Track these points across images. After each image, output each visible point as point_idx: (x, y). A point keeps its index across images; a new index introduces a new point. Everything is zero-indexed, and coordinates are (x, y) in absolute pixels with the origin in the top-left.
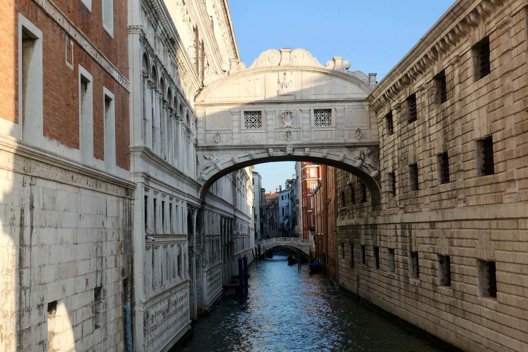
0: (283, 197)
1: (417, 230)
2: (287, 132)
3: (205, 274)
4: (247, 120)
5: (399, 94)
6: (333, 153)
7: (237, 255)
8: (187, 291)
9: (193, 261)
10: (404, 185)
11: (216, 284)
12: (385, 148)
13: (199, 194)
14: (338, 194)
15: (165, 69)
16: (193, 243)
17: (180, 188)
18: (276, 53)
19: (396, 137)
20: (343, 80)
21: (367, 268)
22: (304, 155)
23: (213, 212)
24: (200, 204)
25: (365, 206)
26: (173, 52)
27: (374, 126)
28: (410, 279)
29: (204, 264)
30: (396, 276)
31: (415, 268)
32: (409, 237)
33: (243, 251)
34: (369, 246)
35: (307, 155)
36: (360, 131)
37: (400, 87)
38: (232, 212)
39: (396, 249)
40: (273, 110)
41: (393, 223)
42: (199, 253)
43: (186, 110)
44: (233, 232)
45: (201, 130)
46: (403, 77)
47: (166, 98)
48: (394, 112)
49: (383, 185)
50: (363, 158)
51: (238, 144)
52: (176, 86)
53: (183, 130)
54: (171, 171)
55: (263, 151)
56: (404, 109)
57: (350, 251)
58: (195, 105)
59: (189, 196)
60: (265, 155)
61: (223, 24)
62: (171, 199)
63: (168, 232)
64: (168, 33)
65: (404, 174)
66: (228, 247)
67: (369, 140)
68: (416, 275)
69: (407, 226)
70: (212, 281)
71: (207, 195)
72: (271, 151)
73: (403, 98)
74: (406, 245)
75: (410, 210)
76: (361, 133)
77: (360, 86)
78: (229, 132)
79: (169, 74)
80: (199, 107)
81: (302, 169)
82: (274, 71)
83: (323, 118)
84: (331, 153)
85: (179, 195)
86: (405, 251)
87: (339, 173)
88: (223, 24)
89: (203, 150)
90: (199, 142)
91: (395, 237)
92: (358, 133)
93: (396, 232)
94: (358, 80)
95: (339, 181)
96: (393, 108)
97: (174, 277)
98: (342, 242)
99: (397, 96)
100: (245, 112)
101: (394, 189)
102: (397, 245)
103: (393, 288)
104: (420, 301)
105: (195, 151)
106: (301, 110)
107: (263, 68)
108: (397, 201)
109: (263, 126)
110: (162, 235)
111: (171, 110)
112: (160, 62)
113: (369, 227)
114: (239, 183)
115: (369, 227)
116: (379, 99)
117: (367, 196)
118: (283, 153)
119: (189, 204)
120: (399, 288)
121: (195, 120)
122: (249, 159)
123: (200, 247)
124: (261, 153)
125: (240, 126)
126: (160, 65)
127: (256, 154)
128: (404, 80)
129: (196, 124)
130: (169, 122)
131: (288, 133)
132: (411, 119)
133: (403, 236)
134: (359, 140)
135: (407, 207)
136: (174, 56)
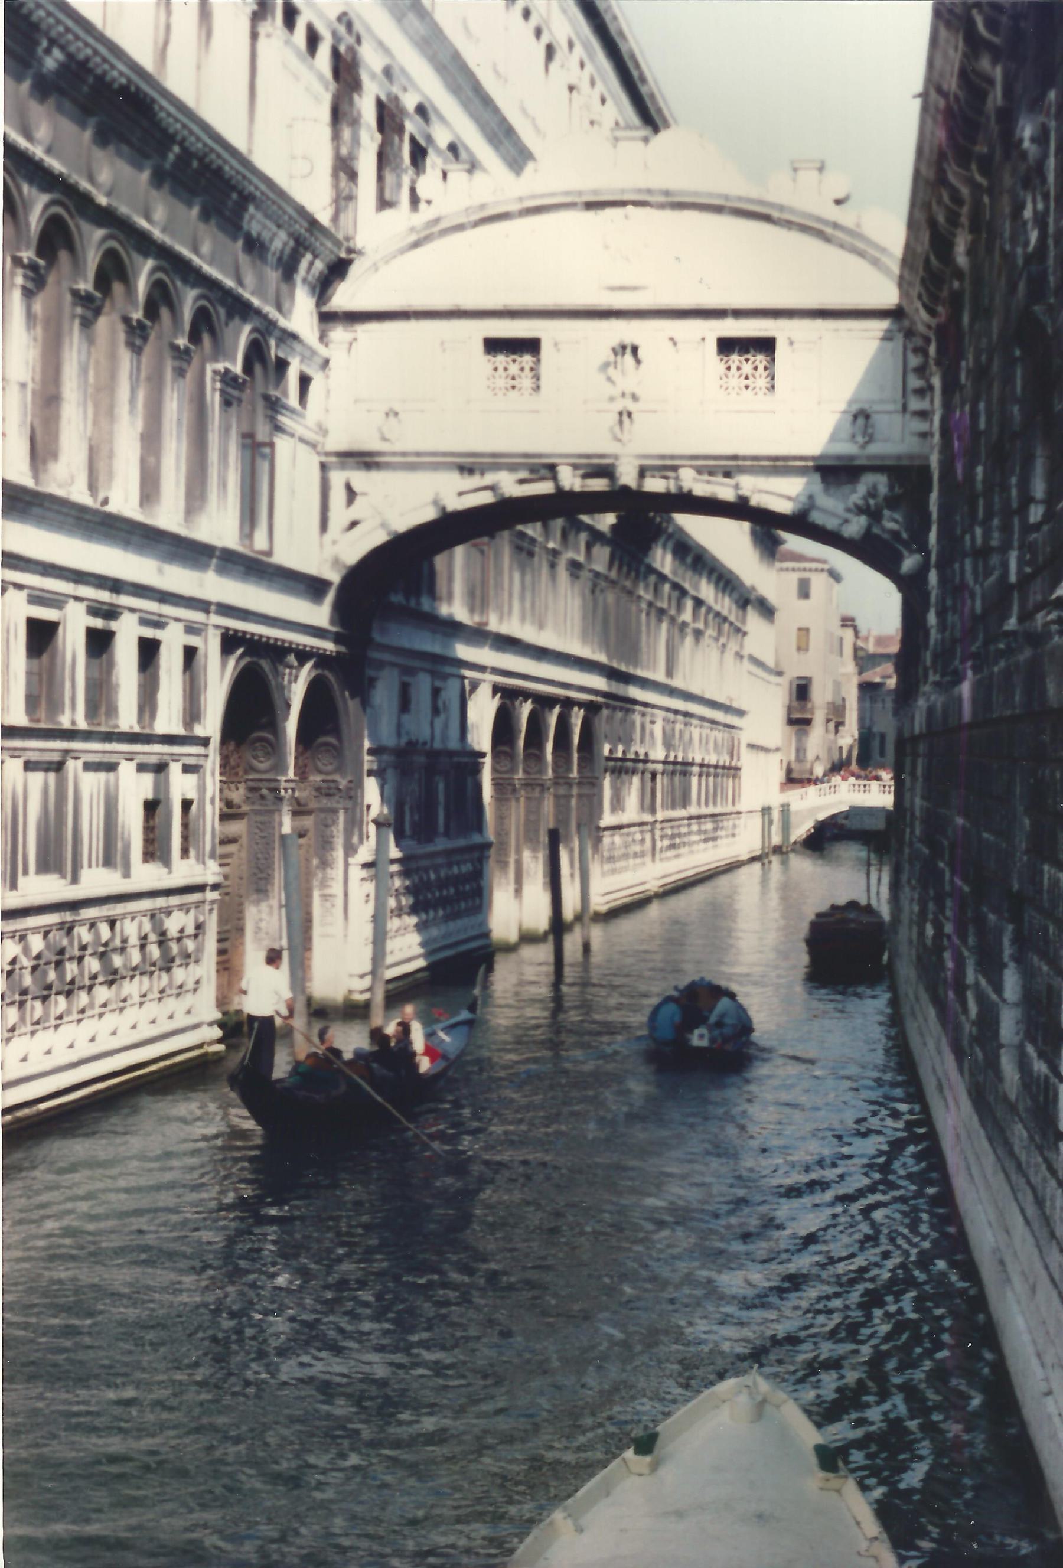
2: (621, 414)
29: (355, 840)
36: (867, 417)
38: (599, 682)
43: (247, 329)
44: (601, 749)
50: (873, 508)
59: (227, 610)
60: (545, 487)
61: (578, 50)
64: (99, 71)
82: (590, 206)
83: (747, 368)
88: (578, 50)
92: (861, 421)
106: (672, 339)
114: (667, 587)
127: (511, 486)
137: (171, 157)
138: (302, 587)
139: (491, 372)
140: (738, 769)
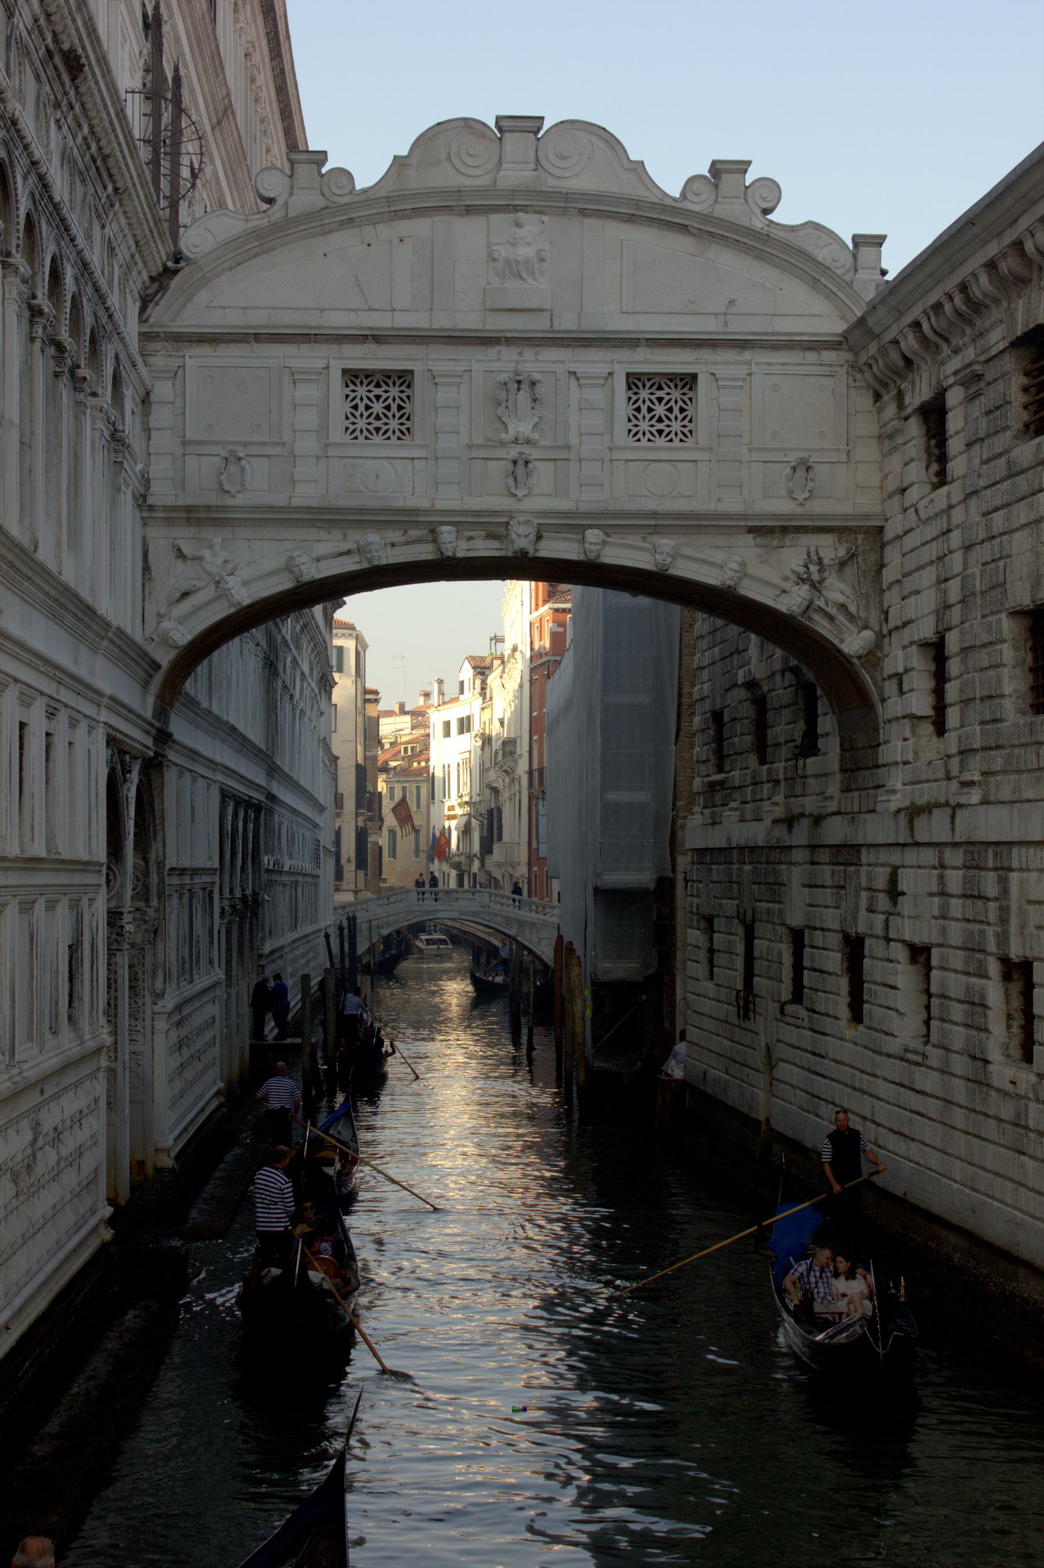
0: (447, 725)
1: (1035, 874)
2: (515, 462)
3: (161, 1025)
4: (356, 407)
5: (979, 322)
6: (698, 555)
7: (272, 952)
8: (99, 1088)
9: (120, 971)
10: (986, 693)
11: (199, 1066)
12: (909, 542)
13: (151, 700)
14: (697, 720)
15: (41, 177)
16: (120, 896)
17: (83, 673)
18: (483, 136)
19: (957, 496)
20: (750, 259)
21: (810, 1019)
22: (582, 557)
23: (196, 776)
24: (150, 742)
25: (809, 772)
26: (71, 107)
27: (868, 452)
28: (991, 1067)
29: (159, 984)
30: (935, 1056)
31: (1015, 1023)
32: (996, 899)
33: (296, 935)
34: (822, 929)
35: (592, 556)
36: (808, 469)
37: (985, 295)
38: (260, 777)
39: (939, 945)
40: (459, 367)
41: (929, 844)
42: (139, 938)
43: (111, 354)
45: (162, 441)
46: (1004, 256)
47: (42, 300)
48: (954, 397)
49: (890, 688)
50: (816, 577)
51: (314, 503)
52: (79, 253)
53: (98, 434)
54: (56, 601)
55: (414, 533)
56: (1000, 385)
57: (740, 948)
58: (145, 337)
59: (116, 705)
60: (424, 552)
62: (51, 715)
63: (39, 849)
64: (59, 28)
65: (984, 646)
66: (243, 918)
67: (846, 508)
68: (1016, 1053)
69: (990, 855)
70: (186, 1053)
71: (177, 704)
72: (447, 533)
73: (997, 338)
74: (982, 932)
75: (1005, 794)
76: (811, 475)
77: (815, 283)
78: (278, 450)
79: (57, 198)
80: (159, 345)
81: (536, 614)
82: (469, 210)
83: (660, 410)
84: (688, 551)
85: (80, 699)
86: (979, 956)
87: (702, 637)
89: (169, 522)
90: (155, 487)
91: (936, 899)
92: (801, 474)
93: (941, 878)
94: (812, 259)
95: (701, 668)
96: (951, 380)
97: (54, 1031)
98: (706, 911)
99: (968, 331)
100: (345, 372)
101: (940, 707)
102: (944, 928)
103: (916, 1101)
104: (1031, 1157)
105: (139, 523)
107: (428, 194)
108: (949, 757)
109: (417, 433)
110: (17, 859)
111: (60, 347)
112: (26, 147)
113: (824, 856)
114: (289, 660)
115: (824, 856)
116: (896, 342)
117: (820, 730)
118: (494, 544)
119: (111, 741)
120: (944, 1100)
121: (142, 394)
122: (357, 567)
123: (144, 913)
124: (407, 543)
125: (323, 430)
126: (25, 162)
128: (1009, 265)
129: (146, 414)
130: (52, 398)
131: (521, 464)
132: (1027, 426)
133: (972, 896)
134: (802, 505)
135: (993, 779)
136: (74, 126)
137: (79, 139)
138: (140, 672)
139: (347, 408)
140: (318, 877)
